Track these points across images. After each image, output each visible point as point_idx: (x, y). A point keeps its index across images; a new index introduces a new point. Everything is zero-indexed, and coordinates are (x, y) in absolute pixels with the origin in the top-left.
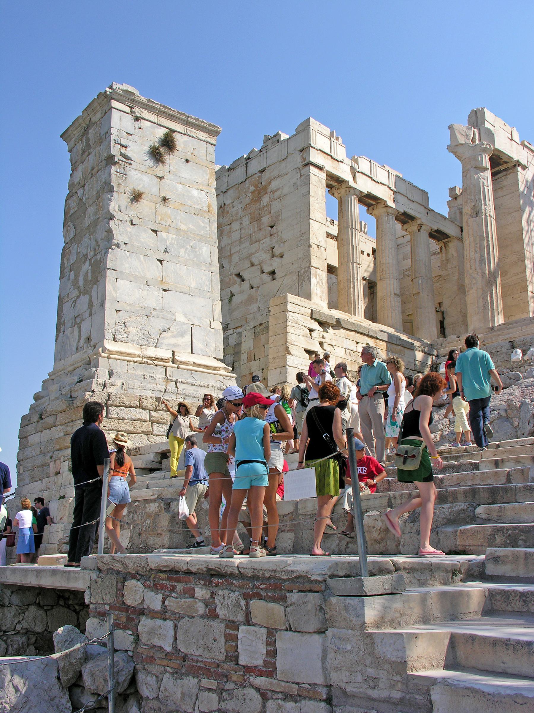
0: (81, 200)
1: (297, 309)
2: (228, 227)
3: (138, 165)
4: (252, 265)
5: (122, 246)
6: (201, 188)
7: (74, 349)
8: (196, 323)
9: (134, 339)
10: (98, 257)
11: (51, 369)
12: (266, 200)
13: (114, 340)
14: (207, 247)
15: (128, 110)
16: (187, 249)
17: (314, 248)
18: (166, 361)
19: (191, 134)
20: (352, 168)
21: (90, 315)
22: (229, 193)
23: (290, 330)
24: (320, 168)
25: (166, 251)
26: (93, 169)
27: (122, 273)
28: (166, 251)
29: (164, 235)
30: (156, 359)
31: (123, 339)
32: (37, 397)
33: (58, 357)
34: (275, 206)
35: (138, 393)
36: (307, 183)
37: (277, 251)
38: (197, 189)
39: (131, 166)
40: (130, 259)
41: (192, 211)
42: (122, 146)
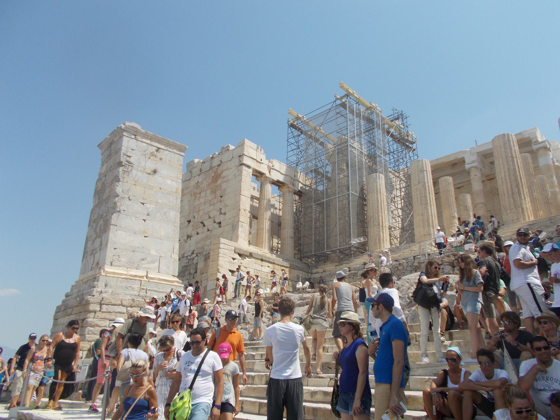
0: (103, 183)
1: (226, 247)
2: (199, 195)
4: (210, 218)
5: (122, 211)
7: (90, 268)
8: (163, 255)
10: (108, 217)
11: (77, 279)
12: (219, 181)
13: (111, 265)
17: (242, 211)
18: (142, 277)
20: (268, 166)
21: (100, 250)
22: (201, 175)
23: (220, 259)
24: (249, 167)
25: (148, 215)
26: (111, 167)
28: (148, 215)
29: (148, 205)
30: (136, 276)
32: (67, 296)
33: (82, 272)
34: (224, 186)
35: (121, 297)
36: (241, 175)
37: (223, 211)
42: (128, 156)
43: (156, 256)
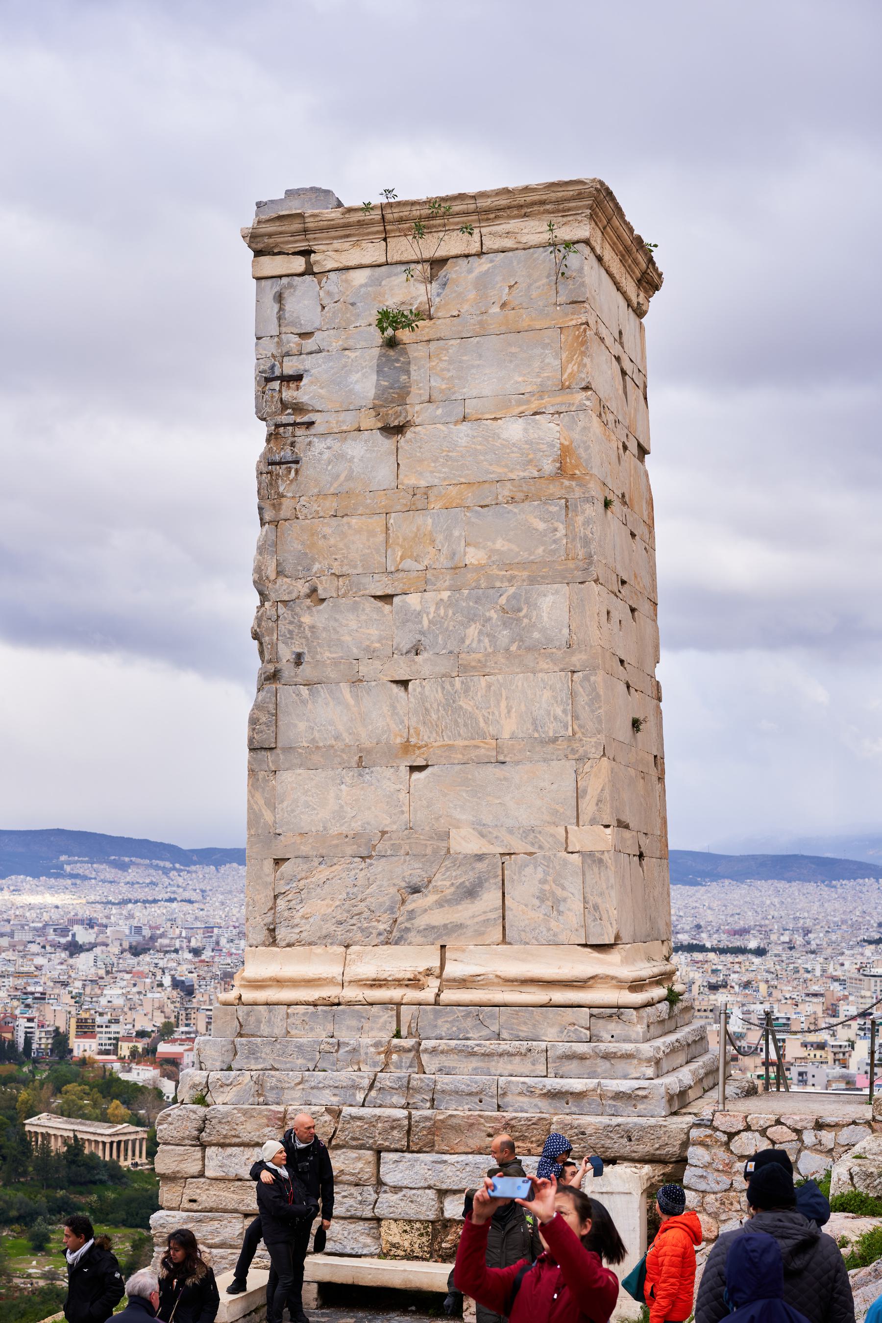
3: (332, 418)
6: (534, 406)
8: (518, 845)
9: (324, 932)
14: (557, 592)
15: (299, 264)
16: (490, 619)
19: (498, 244)
27: (289, 749)
29: (413, 600)
30: (377, 983)
31: (293, 937)
38: (520, 415)
39: (313, 430)
40: (310, 706)
41: (505, 492)
43: (480, 857)
